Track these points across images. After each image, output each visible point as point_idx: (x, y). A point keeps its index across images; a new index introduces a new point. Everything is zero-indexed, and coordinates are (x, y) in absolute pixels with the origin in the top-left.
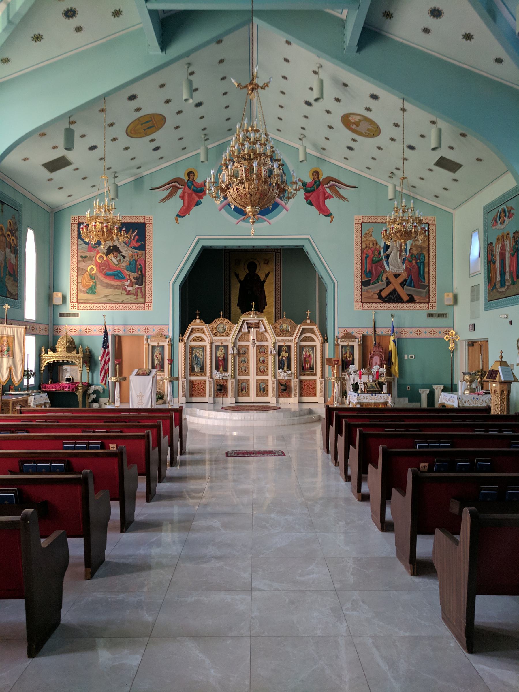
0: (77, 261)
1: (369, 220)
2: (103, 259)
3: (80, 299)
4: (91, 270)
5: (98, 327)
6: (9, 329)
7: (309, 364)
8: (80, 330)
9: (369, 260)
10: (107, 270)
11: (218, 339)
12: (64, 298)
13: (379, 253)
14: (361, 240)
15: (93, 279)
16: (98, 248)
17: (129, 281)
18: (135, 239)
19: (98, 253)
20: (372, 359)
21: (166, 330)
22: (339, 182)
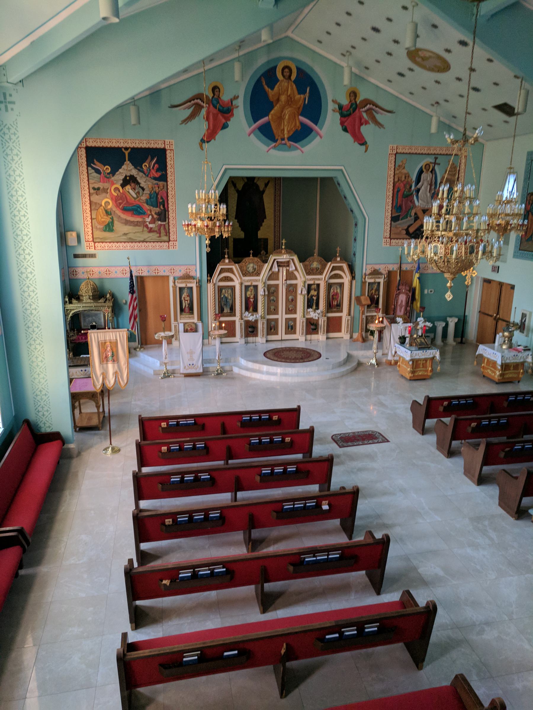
0: (88, 194)
1: (404, 151)
2: (119, 191)
3: (96, 238)
4: (106, 204)
5: (119, 268)
6: (111, 334)
7: (336, 302)
8: (100, 273)
9: (400, 194)
10: (125, 204)
11: (248, 280)
12: (79, 237)
13: (411, 187)
14: (394, 172)
15: (109, 215)
16: (113, 178)
17: (150, 217)
18: (155, 168)
19: (113, 184)
20: (398, 297)
21: (194, 271)
22: (377, 106)
